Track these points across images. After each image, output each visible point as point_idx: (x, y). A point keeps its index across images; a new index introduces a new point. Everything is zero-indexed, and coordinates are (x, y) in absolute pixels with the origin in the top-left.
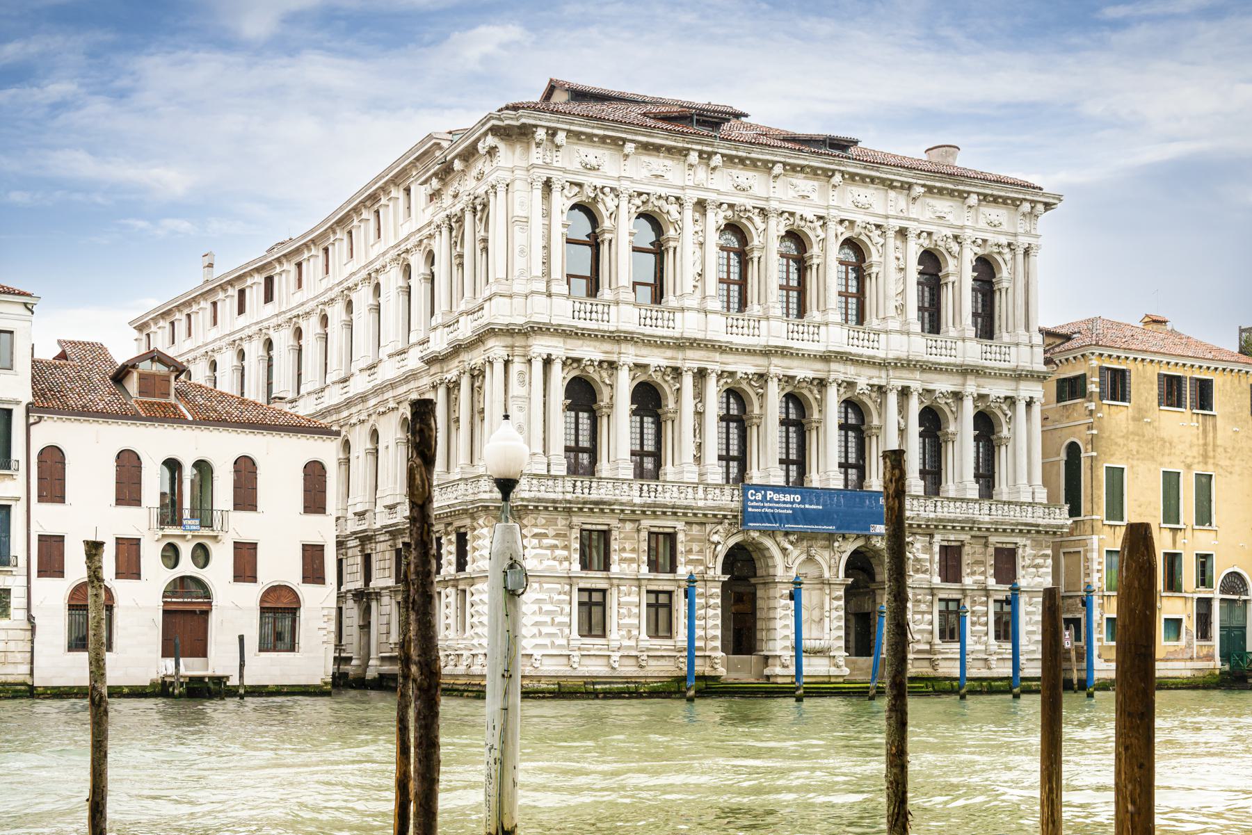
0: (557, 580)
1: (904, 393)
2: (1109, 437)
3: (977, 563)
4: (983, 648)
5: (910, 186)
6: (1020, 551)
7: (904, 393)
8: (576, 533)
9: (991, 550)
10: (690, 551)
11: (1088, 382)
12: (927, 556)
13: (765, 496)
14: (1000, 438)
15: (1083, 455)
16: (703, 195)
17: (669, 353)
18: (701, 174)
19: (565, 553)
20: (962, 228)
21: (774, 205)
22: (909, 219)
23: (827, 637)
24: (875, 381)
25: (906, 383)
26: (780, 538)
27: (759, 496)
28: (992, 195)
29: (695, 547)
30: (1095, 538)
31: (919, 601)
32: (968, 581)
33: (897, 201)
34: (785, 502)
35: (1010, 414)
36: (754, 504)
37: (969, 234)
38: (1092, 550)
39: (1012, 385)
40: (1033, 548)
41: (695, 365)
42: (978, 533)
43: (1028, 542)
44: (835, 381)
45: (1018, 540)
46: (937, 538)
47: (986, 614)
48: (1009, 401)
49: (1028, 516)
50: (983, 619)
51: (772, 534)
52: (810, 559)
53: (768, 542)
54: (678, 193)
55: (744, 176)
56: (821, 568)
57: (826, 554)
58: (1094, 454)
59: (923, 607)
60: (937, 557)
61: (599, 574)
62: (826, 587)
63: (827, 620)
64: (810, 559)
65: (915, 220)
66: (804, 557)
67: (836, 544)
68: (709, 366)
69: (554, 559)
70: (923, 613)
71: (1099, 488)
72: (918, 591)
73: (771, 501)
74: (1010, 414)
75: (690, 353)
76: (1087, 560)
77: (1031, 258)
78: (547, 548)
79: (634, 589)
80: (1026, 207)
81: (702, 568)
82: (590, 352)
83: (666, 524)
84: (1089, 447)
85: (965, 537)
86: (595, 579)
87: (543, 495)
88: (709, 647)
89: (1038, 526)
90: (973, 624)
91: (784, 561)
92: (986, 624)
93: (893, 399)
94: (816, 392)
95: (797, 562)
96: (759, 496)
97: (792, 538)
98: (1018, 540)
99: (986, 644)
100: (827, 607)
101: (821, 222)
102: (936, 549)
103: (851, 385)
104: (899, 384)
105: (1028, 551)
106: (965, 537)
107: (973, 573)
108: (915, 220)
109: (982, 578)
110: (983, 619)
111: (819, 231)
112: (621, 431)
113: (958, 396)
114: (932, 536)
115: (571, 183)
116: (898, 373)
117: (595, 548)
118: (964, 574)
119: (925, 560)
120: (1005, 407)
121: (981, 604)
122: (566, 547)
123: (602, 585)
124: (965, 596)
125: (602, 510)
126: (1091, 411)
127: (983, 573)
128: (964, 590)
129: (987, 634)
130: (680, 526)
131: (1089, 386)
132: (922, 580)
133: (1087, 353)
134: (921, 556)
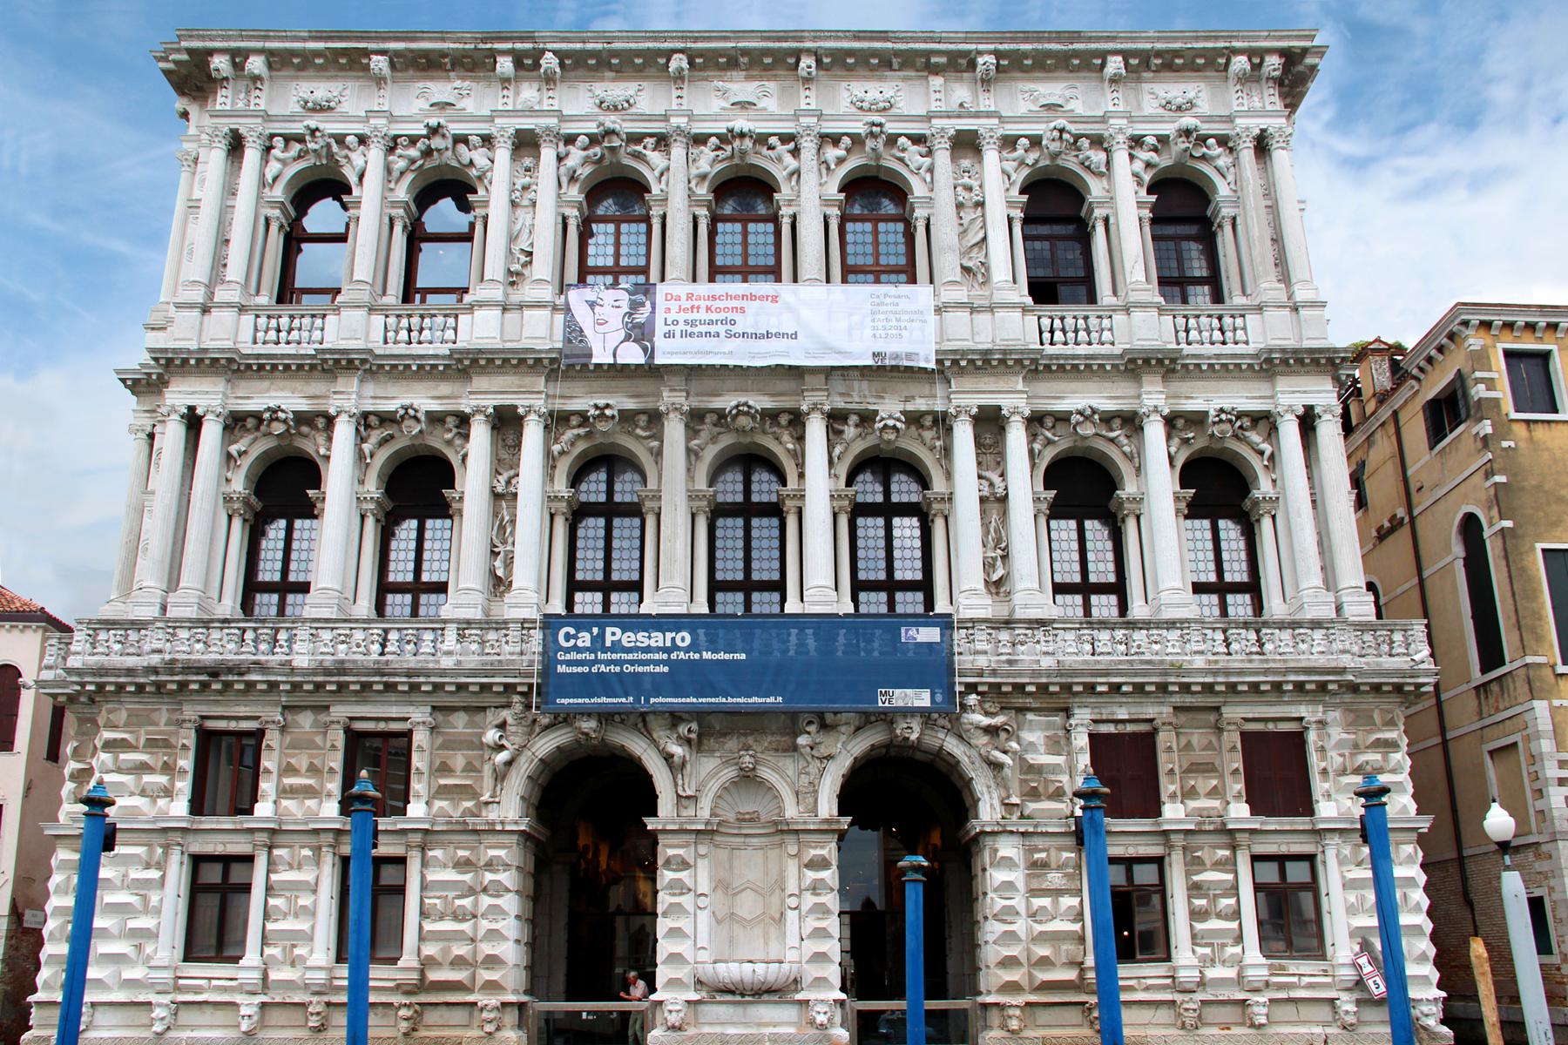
0: (144, 837)
1: (990, 423)
2: (1539, 487)
3: (1195, 768)
4: (1231, 973)
6: (1312, 737)
7: (990, 423)
8: (189, 738)
9: (1233, 738)
10: (445, 769)
11: (1470, 382)
12: (1060, 760)
14: (1256, 503)
15: (1486, 535)
16: (527, 123)
17: (445, 388)
18: (528, 93)
19: (163, 779)
20: (1103, 119)
22: (977, 115)
23: (792, 955)
24: (920, 405)
26: (660, 734)
27: (585, 639)
28: (1158, 54)
29: (459, 761)
30: (1540, 707)
31: (1044, 865)
32: (1173, 812)
33: (961, 92)
34: (648, 650)
35: (1267, 448)
36: (573, 656)
37: (1118, 129)
38: (1538, 735)
39: (1262, 388)
40: (1349, 726)
41: (490, 402)
42: (1188, 700)
43: (1334, 715)
44: (814, 408)
45: (1302, 710)
46: (1082, 716)
47: (1234, 890)
48: (1262, 425)
49: (1315, 652)
50: (1227, 902)
51: (641, 722)
52: (748, 779)
53: (637, 746)
54: (484, 128)
56: (777, 797)
57: (789, 765)
58: (1508, 524)
59: (1055, 879)
60: (1084, 760)
61: (227, 823)
62: (790, 839)
63: (792, 916)
64: (748, 779)
65: (989, 115)
66: (730, 773)
67: (802, 740)
68: (521, 402)
69: (143, 793)
70: (1057, 893)
71: (1533, 595)
72: (1039, 842)
73: (617, 647)
74: (1267, 448)
75: (480, 382)
76: (1534, 759)
77: (1279, 156)
78: (128, 771)
79: (307, 852)
80: (1240, 63)
81: (469, 804)
83: (376, 713)
84: (1495, 512)
85: (1159, 711)
86: (221, 835)
87: (117, 661)
88: (479, 983)
89: (1343, 671)
90: (1196, 915)
91: (687, 788)
92: (1236, 914)
93: (964, 435)
94: (786, 437)
95: (714, 787)
96: (585, 639)
97: (683, 730)
98: (1302, 710)
99: (1238, 961)
100: (792, 887)
101: (792, 145)
102: (1081, 740)
103: (867, 418)
104: (973, 402)
105: (1337, 733)
106: (1159, 711)
107: (1189, 794)
108: (989, 115)
109: (1216, 803)
110: (1227, 902)
111: (788, 159)
112: (334, 542)
113: (1132, 422)
114: (1067, 712)
115: (288, 139)
116: (968, 383)
117: (226, 769)
118: (1164, 797)
119: (1055, 769)
120: (1255, 437)
121: (1219, 865)
122: (168, 768)
123: (239, 847)
124: (1169, 846)
125: (228, 685)
126: (1485, 439)
127: (1213, 793)
128: (1166, 833)
129: (1239, 939)
130: (419, 714)
131: (1473, 392)
132: (1050, 814)
133: (1455, 327)
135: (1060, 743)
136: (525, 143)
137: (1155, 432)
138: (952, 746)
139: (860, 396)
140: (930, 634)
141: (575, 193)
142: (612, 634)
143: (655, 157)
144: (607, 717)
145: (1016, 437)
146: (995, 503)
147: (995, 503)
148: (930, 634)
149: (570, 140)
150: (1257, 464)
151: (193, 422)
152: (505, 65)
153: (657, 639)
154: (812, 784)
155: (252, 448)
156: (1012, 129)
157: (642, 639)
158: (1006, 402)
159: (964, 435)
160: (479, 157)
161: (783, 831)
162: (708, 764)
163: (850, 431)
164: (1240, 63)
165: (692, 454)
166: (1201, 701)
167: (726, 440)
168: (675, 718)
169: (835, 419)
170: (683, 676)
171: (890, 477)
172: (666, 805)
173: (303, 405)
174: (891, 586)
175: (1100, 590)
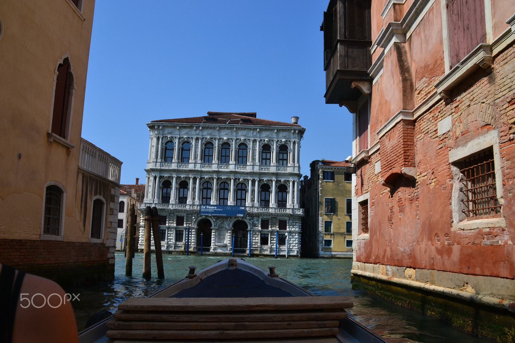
5: (257, 129)
13: (206, 208)
21: (218, 137)
24: (246, 178)
25: (254, 178)
46: (261, 217)
53: (210, 219)
55: (210, 131)
68: (197, 176)
80: (292, 131)
82: (166, 175)
90: (271, 240)
93: (250, 182)
102: (260, 220)
114: (259, 217)
134: (256, 222)
135: (258, 220)
136: (197, 139)
137: (274, 183)
138: (246, 220)
139: (238, 176)
140: (243, 208)
141: (204, 146)
142: (207, 207)
143: (214, 141)
144: (206, 216)
145: (257, 183)
146: (253, 191)
147: (253, 191)
148: (243, 208)
149: (203, 138)
150: (288, 187)
151: (155, 178)
152: (195, 128)
153: (213, 208)
154: (229, 225)
155: (162, 180)
156: (262, 139)
157: (211, 207)
158: (256, 178)
159: (250, 182)
160: (191, 140)
161: (226, 229)
162: (218, 221)
163: (237, 181)
164: (292, 131)
165: (217, 183)
166: (274, 217)
167: (222, 181)
168: (214, 216)
169: (235, 180)
170: (215, 212)
171: (241, 188)
172: (213, 226)
173: (169, 175)
174: (241, 199)
175: (265, 203)
